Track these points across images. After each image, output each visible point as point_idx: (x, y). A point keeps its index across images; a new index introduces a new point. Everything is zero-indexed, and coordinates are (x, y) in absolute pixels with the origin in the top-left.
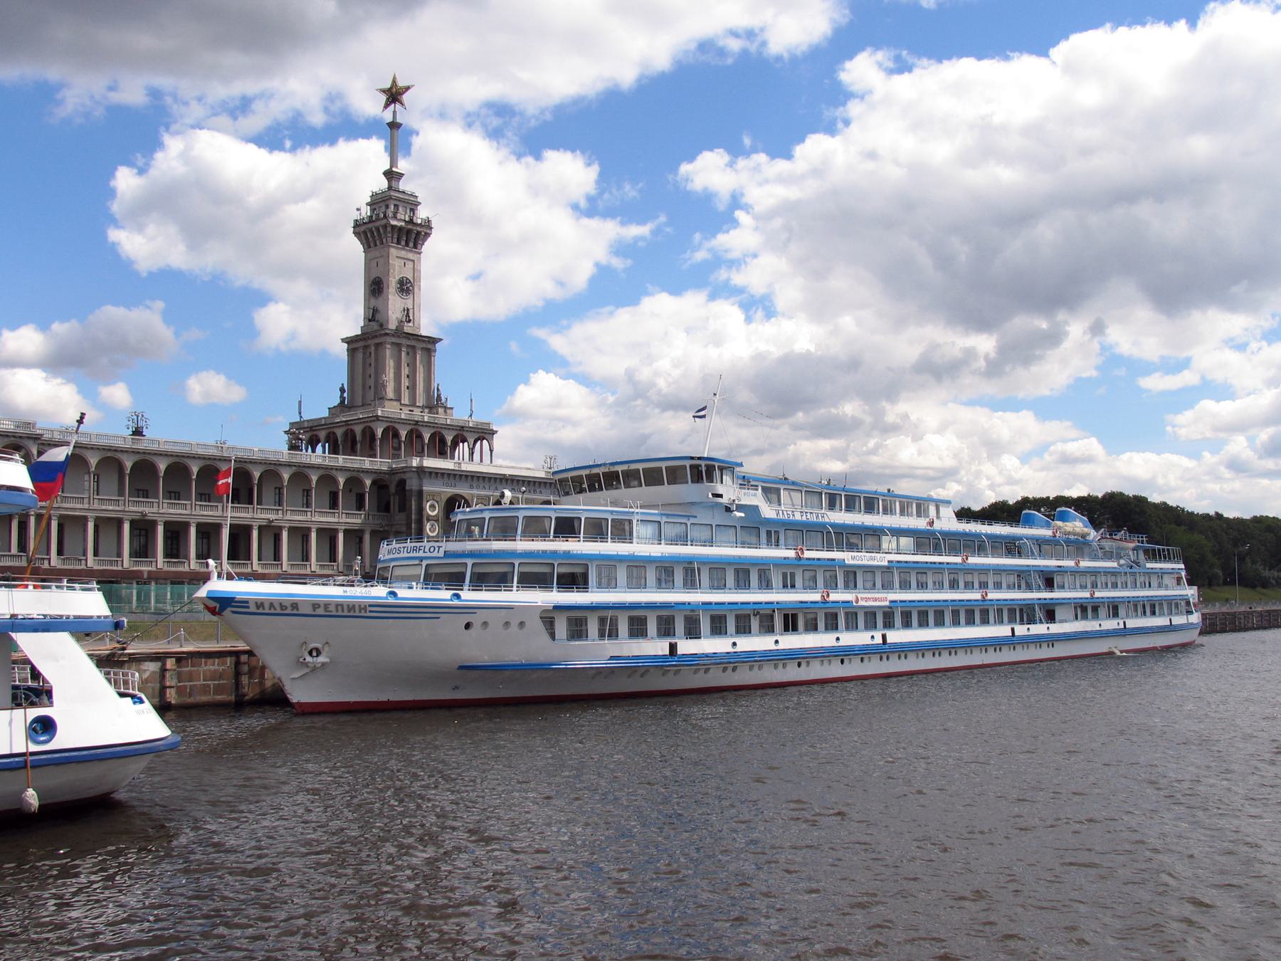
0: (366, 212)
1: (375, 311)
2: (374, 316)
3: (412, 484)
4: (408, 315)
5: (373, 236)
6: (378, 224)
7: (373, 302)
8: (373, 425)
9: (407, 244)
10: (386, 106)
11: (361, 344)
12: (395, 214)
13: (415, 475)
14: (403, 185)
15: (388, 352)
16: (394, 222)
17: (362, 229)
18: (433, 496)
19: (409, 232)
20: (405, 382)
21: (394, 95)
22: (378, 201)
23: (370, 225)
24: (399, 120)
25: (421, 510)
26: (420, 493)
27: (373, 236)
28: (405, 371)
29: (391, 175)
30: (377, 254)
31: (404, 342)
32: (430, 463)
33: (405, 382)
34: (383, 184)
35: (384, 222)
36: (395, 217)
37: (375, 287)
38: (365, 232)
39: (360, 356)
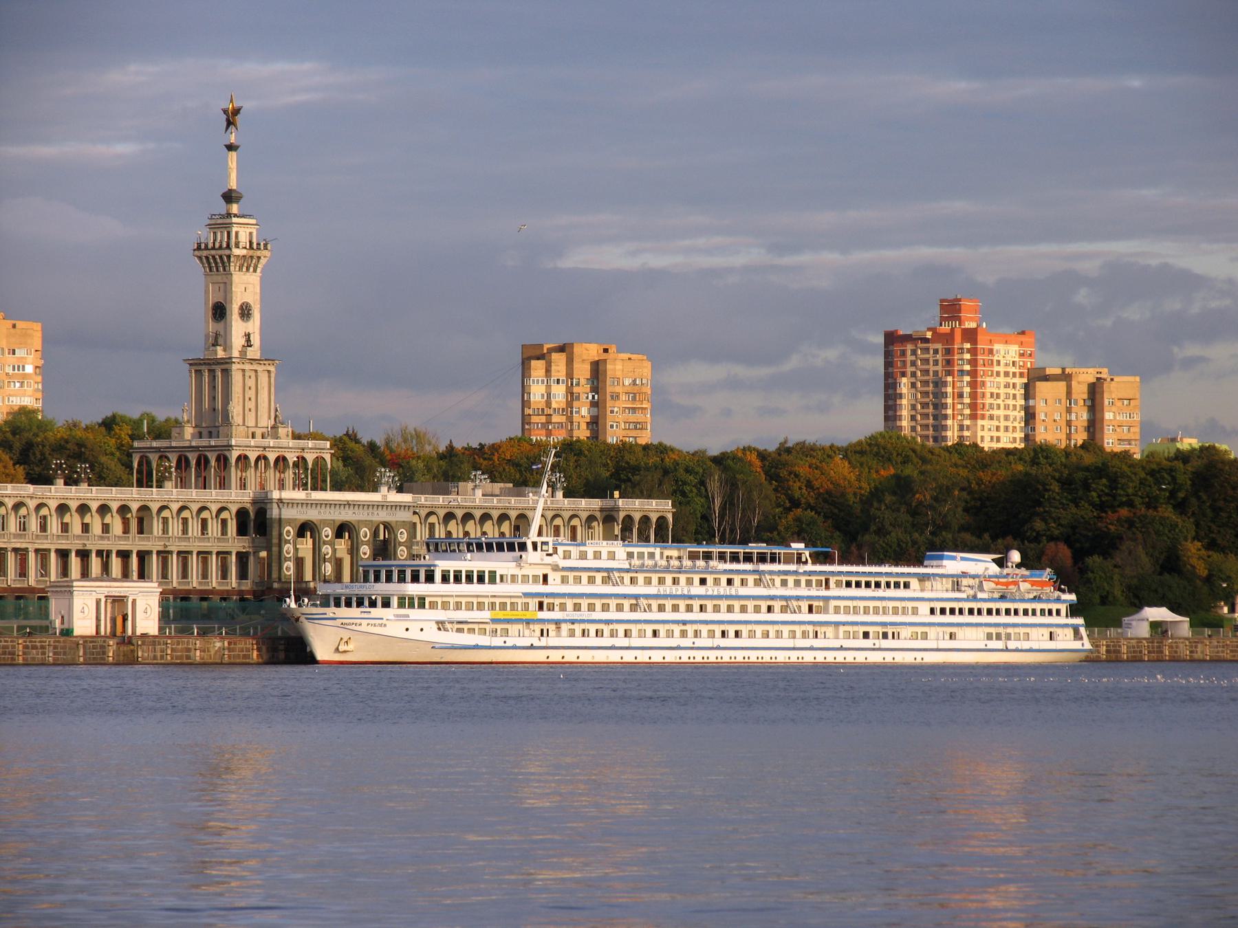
1: (217, 335)
3: (274, 512)
4: (248, 340)
5: (216, 263)
6: (220, 252)
8: (227, 453)
9: (248, 269)
12: (237, 246)
13: (275, 506)
15: (236, 378)
16: (236, 252)
18: (290, 522)
19: (252, 257)
21: (232, 116)
23: (213, 252)
25: (280, 535)
27: (216, 263)
28: (251, 393)
31: (247, 367)
32: (289, 494)
33: (251, 405)
35: (227, 252)
36: (237, 246)
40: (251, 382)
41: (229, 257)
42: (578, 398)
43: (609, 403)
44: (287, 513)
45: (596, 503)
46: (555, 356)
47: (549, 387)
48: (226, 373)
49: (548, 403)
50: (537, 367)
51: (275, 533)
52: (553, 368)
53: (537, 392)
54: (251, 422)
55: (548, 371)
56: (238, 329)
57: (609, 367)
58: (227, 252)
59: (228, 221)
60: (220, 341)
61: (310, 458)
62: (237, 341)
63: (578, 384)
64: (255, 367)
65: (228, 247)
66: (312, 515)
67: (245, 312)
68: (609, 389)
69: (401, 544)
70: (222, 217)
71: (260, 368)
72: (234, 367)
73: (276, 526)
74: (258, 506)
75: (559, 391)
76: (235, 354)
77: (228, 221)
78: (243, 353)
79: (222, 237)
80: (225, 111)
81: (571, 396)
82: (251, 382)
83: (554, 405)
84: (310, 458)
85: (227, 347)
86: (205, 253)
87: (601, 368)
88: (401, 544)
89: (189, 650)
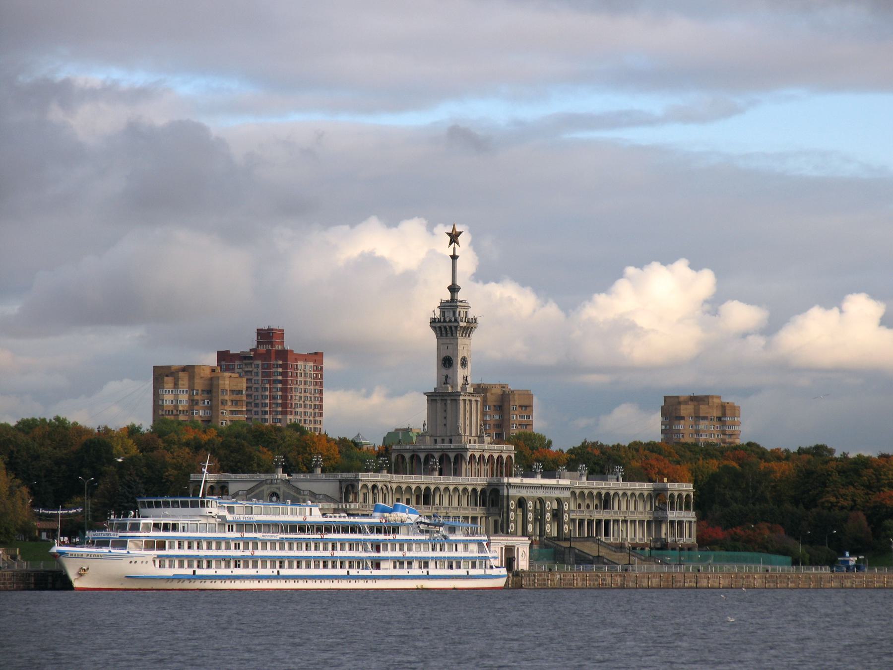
0: (438, 314)
1: (447, 377)
2: (446, 380)
7: (444, 372)
10: (450, 244)
11: (437, 398)
14: (460, 296)
15: (462, 403)
17: (439, 325)
18: (513, 498)
20: (468, 422)
22: (443, 307)
23: (445, 324)
24: (457, 254)
26: (508, 496)
29: (453, 289)
30: (448, 341)
31: (467, 398)
33: (468, 422)
34: (447, 296)
35: (456, 324)
37: (447, 362)
38: (440, 327)
39: (439, 405)
40: (468, 408)
41: (456, 327)
42: (197, 404)
43: (221, 407)
44: (513, 492)
45: (647, 486)
46: (181, 374)
47: (176, 396)
48: (456, 401)
49: (176, 407)
50: (169, 382)
51: (505, 505)
52: (180, 382)
53: (168, 398)
54: (468, 433)
55: (176, 385)
56: (461, 373)
57: (221, 382)
58: (456, 324)
59: (454, 304)
60: (449, 381)
61: (505, 456)
62: (460, 381)
63: (197, 394)
64: (470, 398)
65: (456, 321)
66: (524, 493)
67: (464, 363)
68: (221, 398)
69: (565, 512)
70: (448, 301)
71: (473, 399)
72: (461, 398)
73: (505, 500)
74: (492, 488)
75: (184, 398)
76: (459, 390)
77: (454, 304)
78: (464, 388)
79: (449, 315)
80: (449, 234)
81: (193, 402)
82: (468, 408)
83: (180, 408)
84: (505, 456)
85: (454, 385)
86: (439, 325)
87: (215, 383)
88: (565, 512)
89: (544, 580)
